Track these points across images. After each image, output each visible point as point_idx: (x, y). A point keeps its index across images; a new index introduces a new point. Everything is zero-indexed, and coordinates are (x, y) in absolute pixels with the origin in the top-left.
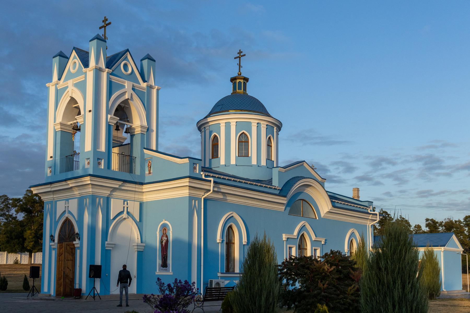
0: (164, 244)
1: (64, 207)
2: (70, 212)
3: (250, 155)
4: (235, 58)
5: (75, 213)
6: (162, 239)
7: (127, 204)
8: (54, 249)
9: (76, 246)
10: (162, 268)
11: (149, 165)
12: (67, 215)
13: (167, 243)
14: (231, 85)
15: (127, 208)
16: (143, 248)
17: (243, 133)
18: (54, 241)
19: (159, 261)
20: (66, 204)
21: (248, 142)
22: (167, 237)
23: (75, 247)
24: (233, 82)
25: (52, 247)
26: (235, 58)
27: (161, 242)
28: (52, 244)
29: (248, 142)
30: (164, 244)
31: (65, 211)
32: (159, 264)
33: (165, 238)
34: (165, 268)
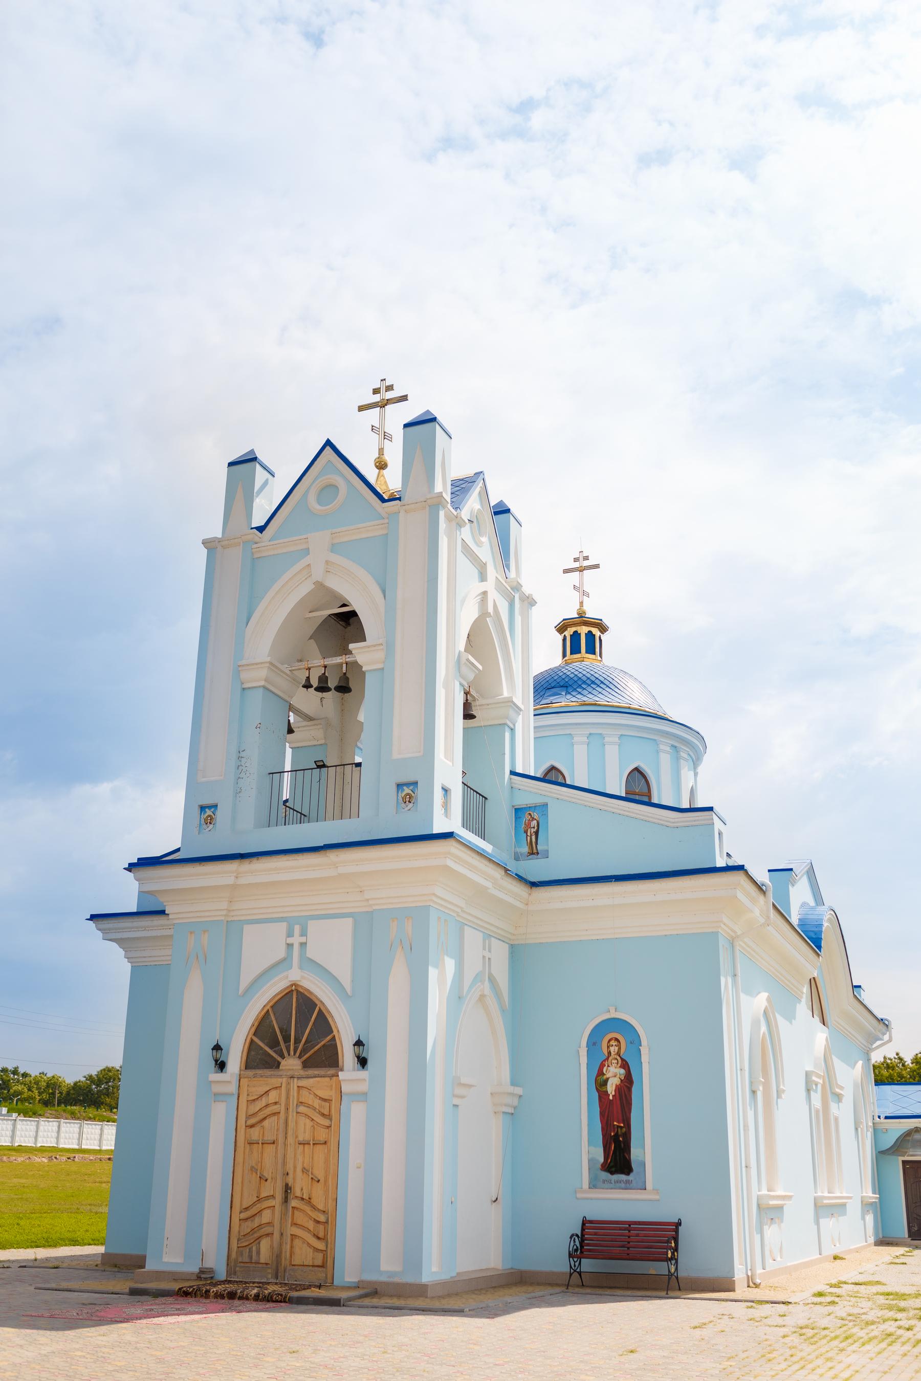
0: (611, 1089)
1: (284, 947)
5: (342, 969)
9: (345, 1088)
10: (605, 1175)
11: (528, 825)
12: (295, 975)
16: (515, 1102)
17: (637, 769)
19: (589, 1149)
20: (290, 934)
24: (568, 633)
25: (216, 1089)
26: (566, 571)
27: (600, 1084)
28: (220, 1076)
30: (611, 1089)
32: (591, 1161)
34: (623, 1177)
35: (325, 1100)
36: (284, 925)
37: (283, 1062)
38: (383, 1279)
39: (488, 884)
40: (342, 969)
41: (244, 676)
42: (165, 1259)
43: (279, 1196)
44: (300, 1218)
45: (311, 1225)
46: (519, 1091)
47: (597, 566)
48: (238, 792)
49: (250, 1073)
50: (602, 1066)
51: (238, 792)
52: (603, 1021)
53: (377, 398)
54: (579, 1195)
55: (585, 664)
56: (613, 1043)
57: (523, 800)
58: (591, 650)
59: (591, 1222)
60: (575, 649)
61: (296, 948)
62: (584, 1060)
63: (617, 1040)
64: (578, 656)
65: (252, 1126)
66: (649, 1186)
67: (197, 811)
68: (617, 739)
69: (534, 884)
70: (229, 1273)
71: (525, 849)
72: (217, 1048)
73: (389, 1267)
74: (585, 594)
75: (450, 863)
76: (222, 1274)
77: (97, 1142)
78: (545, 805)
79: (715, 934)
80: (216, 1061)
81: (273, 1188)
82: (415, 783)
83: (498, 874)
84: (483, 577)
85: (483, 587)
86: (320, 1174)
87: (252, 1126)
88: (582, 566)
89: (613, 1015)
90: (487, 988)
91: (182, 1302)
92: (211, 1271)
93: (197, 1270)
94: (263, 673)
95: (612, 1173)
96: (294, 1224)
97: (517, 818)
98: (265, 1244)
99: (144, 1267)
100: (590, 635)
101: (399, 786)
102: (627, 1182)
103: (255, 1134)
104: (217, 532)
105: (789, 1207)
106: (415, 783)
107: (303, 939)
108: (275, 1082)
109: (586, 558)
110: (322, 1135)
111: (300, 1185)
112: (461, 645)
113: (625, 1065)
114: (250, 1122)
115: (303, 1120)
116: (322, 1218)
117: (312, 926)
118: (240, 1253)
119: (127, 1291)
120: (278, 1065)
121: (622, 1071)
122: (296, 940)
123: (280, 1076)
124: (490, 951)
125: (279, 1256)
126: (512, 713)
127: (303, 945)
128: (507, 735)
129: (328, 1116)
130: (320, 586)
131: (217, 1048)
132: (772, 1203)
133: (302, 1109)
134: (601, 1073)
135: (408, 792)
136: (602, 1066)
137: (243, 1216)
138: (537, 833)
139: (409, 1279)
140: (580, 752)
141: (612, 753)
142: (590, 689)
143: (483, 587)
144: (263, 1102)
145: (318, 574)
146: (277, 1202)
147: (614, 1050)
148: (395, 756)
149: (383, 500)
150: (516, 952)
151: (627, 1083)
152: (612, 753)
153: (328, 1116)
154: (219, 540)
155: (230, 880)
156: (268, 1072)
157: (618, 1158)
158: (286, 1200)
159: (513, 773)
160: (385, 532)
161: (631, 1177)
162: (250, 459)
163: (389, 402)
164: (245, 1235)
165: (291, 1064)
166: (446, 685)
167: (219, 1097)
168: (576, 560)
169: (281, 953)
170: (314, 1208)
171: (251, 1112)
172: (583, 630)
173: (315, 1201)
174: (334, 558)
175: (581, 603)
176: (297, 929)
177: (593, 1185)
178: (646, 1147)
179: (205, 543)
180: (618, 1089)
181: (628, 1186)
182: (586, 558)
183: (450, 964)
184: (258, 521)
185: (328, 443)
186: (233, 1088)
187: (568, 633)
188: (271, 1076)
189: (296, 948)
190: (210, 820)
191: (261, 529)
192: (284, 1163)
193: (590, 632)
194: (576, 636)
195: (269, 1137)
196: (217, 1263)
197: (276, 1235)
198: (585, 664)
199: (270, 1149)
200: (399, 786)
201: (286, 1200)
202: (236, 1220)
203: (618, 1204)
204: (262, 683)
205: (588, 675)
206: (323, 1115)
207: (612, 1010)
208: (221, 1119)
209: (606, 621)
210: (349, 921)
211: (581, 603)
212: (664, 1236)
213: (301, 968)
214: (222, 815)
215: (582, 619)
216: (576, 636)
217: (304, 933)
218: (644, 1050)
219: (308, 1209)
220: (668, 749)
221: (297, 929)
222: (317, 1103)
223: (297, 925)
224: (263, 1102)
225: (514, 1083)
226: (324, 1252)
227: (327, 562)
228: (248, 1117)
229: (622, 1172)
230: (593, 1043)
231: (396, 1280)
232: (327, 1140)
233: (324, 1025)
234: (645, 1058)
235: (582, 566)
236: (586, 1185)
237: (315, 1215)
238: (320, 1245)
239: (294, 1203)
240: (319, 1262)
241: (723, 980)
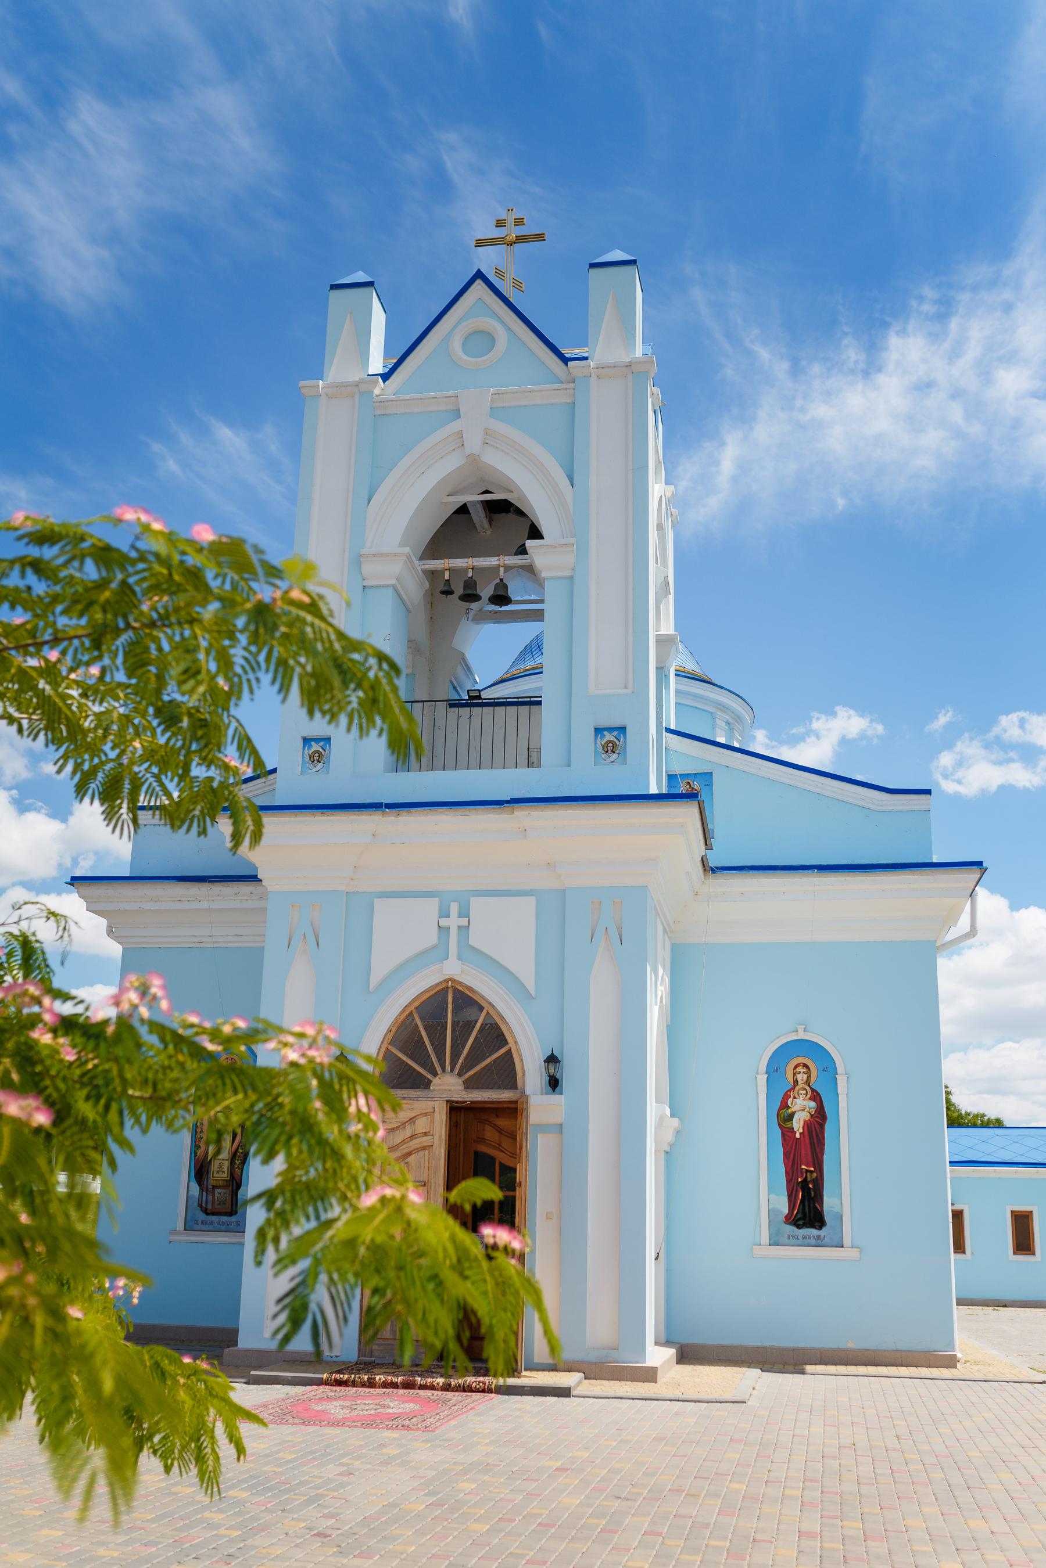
0: (798, 1125)
6: (784, 1105)
10: (791, 1229)
12: (454, 969)
13: (822, 1126)
20: (445, 914)
22: (816, 1096)
27: (784, 1118)
30: (798, 1125)
36: (432, 905)
41: (367, 568)
50: (786, 1096)
56: (800, 1069)
61: (453, 933)
63: (805, 1066)
66: (847, 1242)
82: (623, 729)
89: (801, 1035)
95: (799, 1227)
99: (235, 1343)
101: (599, 731)
106: (623, 729)
107: (464, 922)
113: (816, 1096)
117: (477, 905)
120: (426, 1084)
121: (813, 1104)
122: (453, 922)
123: (432, 1099)
127: (464, 930)
130: (474, 460)
134: (784, 1105)
135: (612, 740)
144: (408, 1132)
145: (474, 444)
147: (801, 1078)
151: (819, 1120)
161: (823, 1232)
174: (500, 427)
176: (454, 908)
180: (807, 1125)
181: (820, 1243)
188: (417, 1099)
189: (453, 933)
190: (317, 758)
200: (599, 731)
204: (394, 582)
207: (801, 1029)
217: (465, 913)
218: (841, 1080)
221: (454, 908)
224: (408, 1132)
227: (487, 432)
229: (812, 1226)
230: (774, 1069)
233: (495, 1035)
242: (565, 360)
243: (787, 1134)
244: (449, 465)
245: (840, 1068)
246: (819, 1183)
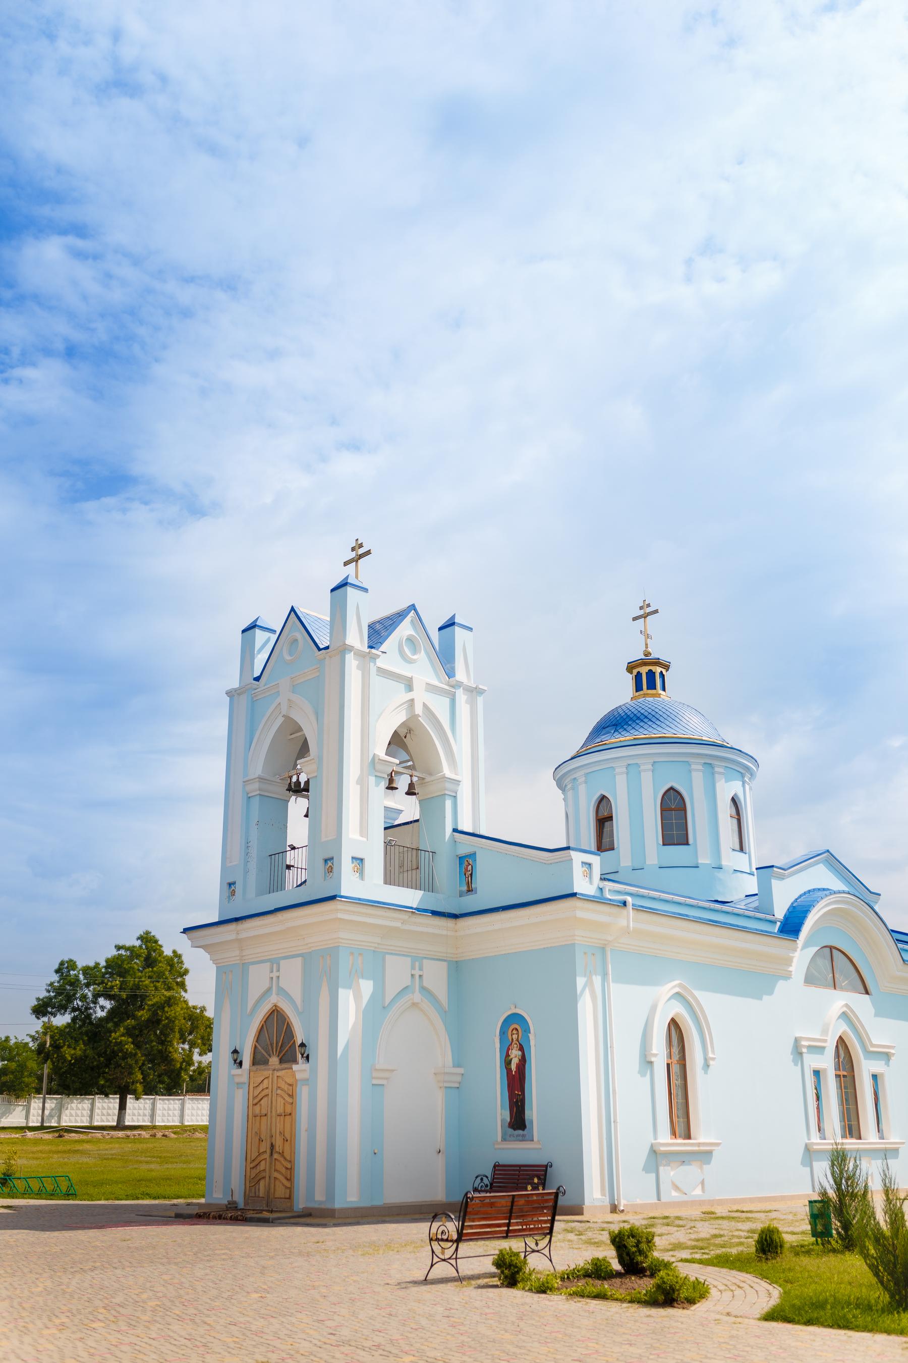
0: (513, 1067)
2: (281, 991)
3: (691, 841)
4: (635, 619)
5: (296, 992)
7: (421, 969)
8: (239, 1085)
9: (298, 1076)
10: (511, 1131)
11: (466, 870)
12: (274, 999)
14: (629, 679)
15: (420, 976)
16: (459, 1079)
17: (672, 788)
18: (241, 1064)
19: (501, 1113)
21: (684, 809)
23: (296, 1081)
24: (635, 672)
25: (237, 1080)
26: (635, 619)
27: (508, 1063)
28: (239, 1071)
29: (685, 810)
30: (513, 1067)
31: (269, 990)
32: (502, 1121)
33: (515, 1054)
34: (520, 1132)
35: (290, 1085)
37: (270, 1060)
38: (316, 1206)
39: (398, 924)
40: (296, 992)
42: (215, 1196)
43: (268, 1151)
44: (279, 1167)
45: (283, 1170)
46: (460, 1070)
47: (656, 612)
48: (246, 872)
49: (254, 1068)
50: (508, 1049)
51: (246, 872)
52: (509, 1016)
53: (353, 555)
54: (496, 1146)
55: (648, 701)
56: (515, 1032)
57: (463, 851)
58: (652, 685)
59: (499, 1166)
60: (638, 688)
62: (498, 1045)
63: (517, 1030)
64: (641, 692)
65: (256, 1104)
66: (535, 1139)
67: (226, 887)
68: (650, 767)
69: (455, 916)
70: (246, 1203)
71: (465, 888)
72: (235, 1052)
73: (319, 1197)
74: (648, 636)
75: (340, 916)
76: (241, 1205)
77: (147, 1118)
78: (475, 853)
79: (574, 944)
80: (235, 1061)
81: (265, 1147)
83: (405, 917)
84: (410, 688)
85: (410, 696)
86: (288, 1136)
87: (256, 1104)
88: (646, 613)
89: (514, 1011)
90: (417, 997)
91: (195, 1221)
92: (235, 1203)
93: (226, 1203)
94: (256, 785)
95: (515, 1129)
96: (275, 1170)
97: (460, 864)
98: (262, 1183)
100: (651, 674)
101: (326, 861)
102: (523, 1136)
103: (257, 1108)
104: (236, 685)
105: (717, 1152)
107: (277, 974)
108: (266, 1073)
109: (649, 605)
110: (288, 1110)
111: (278, 1143)
112: (380, 749)
113: (521, 1048)
114: (256, 1101)
115: (279, 1099)
116: (289, 1166)
117: (282, 963)
118: (250, 1191)
119: (173, 1215)
121: (520, 1053)
122: (275, 974)
123: (269, 1069)
124: (421, 969)
125: (268, 1192)
126: (448, 785)
127: (278, 977)
128: (448, 803)
129: (291, 1096)
131: (235, 1052)
132: (662, 1149)
133: (279, 1092)
134: (508, 1055)
135: (330, 864)
136: (508, 1049)
137: (252, 1165)
138: (471, 875)
139: (328, 1206)
140: (621, 781)
141: (647, 778)
142: (642, 724)
143: (410, 696)
144: (260, 1088)
146: (267, 1156)
147: (515, 1037)
148: (324, 839)
149: (319, 649)
150: (457, 969)
151: (523, 1061)
152: (647, 778)
153: (291, 1096)
154: (236, 690)
155: (233, 936)
156: (262, 1067)
157: (518, 1120)
158: (271, 1154)
159: (455, 830)
160: (318, 674)
161: (525, 1132)
162: (253, 626)
163: (361, 556)
164: (253, 1180)
165: (274, 1060)
166: (361, 781)
167: (239, 1085)
168: (641, 608)
169: (266, 985)
170: (285, 1159)
171: (256, 1094)
172: (644, 670)
173: (285, 1154)
175: (646, 645)
177: (504, 1139)
178: (533, 1112)
179: (228, 693)
180: (518, 1066)
181: (523, 1139)
182: (649, 605)
183: (367, 987)
184: (257, 674)
185: (293, 609)
186: (245, 1079)
187: (635, 672)
188: (265, 1070)
190: (233, 893)
191: (257, 679)
192: (271, 1130)
193: (650, 671)
194: (639, 675)
195: (264, 1112)
196: (239, 1198)
197: (267, 1178)
198: (648, 701)
199: (264, 1119)
200: (326, 861)
201: (271, 1154)
202: (248, 1169)
203: (518, 1153)
204: (258, 792)
205: (650, 711)
206: (289, 1095)
207: (513, 1007)
208: (240, 1099)
209: (664, 657)
210: (299, 961)
211: (646, 645)
212: (527, 1175)
213: (277, 994)
214: (239, 888)
215: (648, 661)
216: (639, 675)
218: (531, 1036)
219: (282, 1159)
220: (700, 767)
222: (286, 1087)
223: (275, 963)
224: (260, 1088)
225: (457, 1065)
226: (290, 1188)
228: (254, 1098)
230: (503, 1033)
231: (323, 1206)
232: (289, 1114)
233: (289, 1032)
234: (532, 1043)
235: (646, 613)
236: (499, 1139)
237: (284, 1163)
238: (288, 1184)
239: (276, 1156)
240: (287, 1196)
241: (580, 981)
242: (319, 649)
243: (509, 1070)
244: (280, 720)
245: (532, 1031)
246: (523, 1101)
